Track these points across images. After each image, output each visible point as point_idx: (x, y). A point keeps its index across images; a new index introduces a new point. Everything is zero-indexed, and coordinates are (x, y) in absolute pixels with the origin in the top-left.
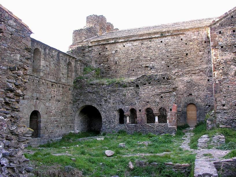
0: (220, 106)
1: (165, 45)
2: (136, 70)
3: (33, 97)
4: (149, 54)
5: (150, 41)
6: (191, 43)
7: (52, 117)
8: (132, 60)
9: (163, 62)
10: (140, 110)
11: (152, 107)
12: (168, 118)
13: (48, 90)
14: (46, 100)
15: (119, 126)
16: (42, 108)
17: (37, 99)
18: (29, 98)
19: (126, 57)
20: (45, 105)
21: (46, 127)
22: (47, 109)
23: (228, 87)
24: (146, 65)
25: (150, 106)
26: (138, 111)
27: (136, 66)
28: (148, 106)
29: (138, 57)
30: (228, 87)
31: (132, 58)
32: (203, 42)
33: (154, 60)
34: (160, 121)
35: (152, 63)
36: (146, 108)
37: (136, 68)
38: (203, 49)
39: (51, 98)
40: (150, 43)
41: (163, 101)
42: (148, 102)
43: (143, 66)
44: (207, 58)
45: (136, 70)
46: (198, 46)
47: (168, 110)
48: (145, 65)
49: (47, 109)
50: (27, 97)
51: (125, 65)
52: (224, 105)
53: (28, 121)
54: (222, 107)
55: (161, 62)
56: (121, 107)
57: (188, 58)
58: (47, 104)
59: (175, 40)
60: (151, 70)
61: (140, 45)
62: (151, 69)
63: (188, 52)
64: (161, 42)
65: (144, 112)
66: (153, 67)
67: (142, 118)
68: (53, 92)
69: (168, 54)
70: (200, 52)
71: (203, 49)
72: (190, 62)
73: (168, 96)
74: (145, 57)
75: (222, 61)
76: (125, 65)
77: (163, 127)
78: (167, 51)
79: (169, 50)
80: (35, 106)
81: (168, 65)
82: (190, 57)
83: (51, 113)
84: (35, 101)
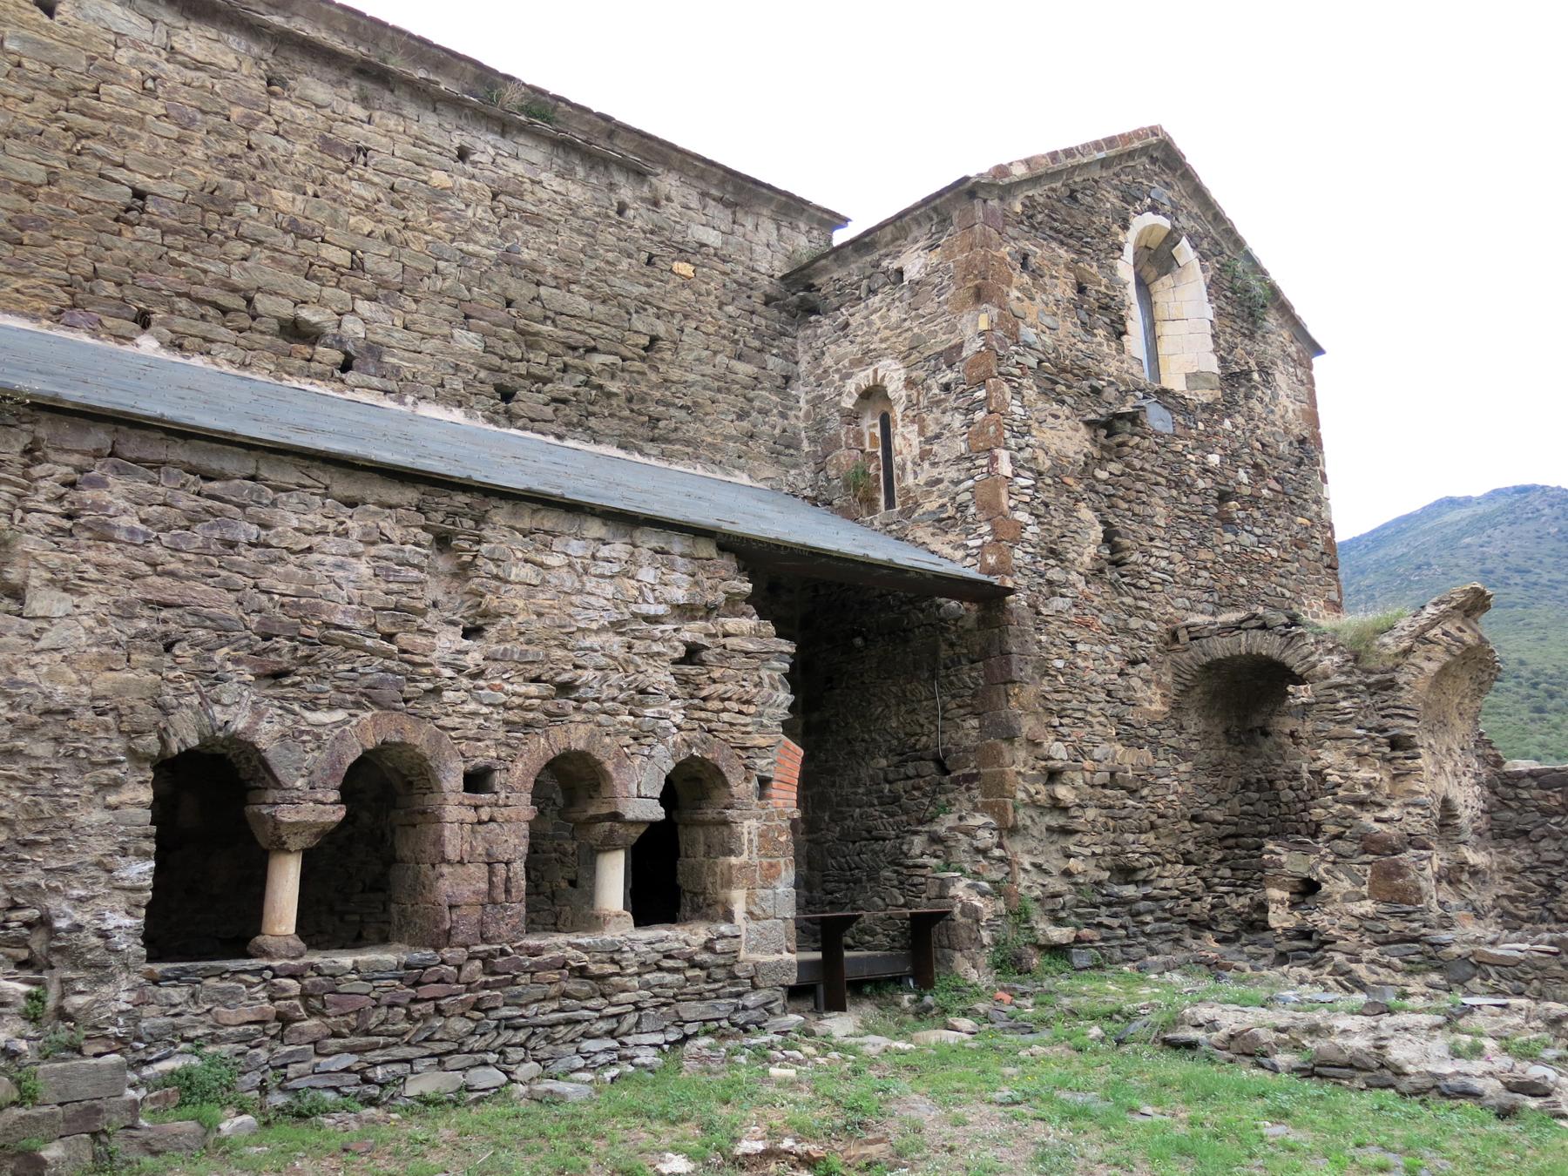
0: (1034, 780)
1: (495, 196)
2: (180, 323)
4: (343, 211)
5: (364, 101)
6: (685, 269)
8: (139, 194)
9: (468, 341)
10: (477, 781)
11: (605, 751)
12: (742, 867)
15: (178, 994)
19: (54, 128)
23: (1073, 643)
24: (306, 314)
25: (592, 735)
26: (452, 780)
27: (172, 279)
28: (575, 736)
29: (211, 198)
30: (1073, 643)
31: (141, 181)
32: (758, 298)
33: (384, 292)
34: (317, 925)
35: (363, 307)
36: (541, 748)
37: (183, 304)
38: (757, 344)
40: (358, 111)
41: (704, 699)
42: (565, 689)
43: (263, 303)
44: (780, 422)
45: (180, 323)
46: (730, 309)
47: (741, 788)
48: (286, 310)
51: (40, 224)
52: (1053, 776)
54: (1040, 786)
55: (446, 330)
56: (243, 711)
57: (653, 377)
59: (577, 193)
60: (351, 377)
61: (257, 86)
62: (346, 367)
63: (661, 328)
64: (463, 154)
65: (522, 808)
66: (374, 350)
67: (501, 869)
69: (513, 283)
70: (739, 357)
71: (757, 344)
72: (672, 411)
73: (751, 647)
74: (296, 229)
75: (1040, 454)
76: (40, 224)
77: (694, 965)
78: (508, 259)
79: (527, 255)
81: (506, 380)
82: (675, 374)
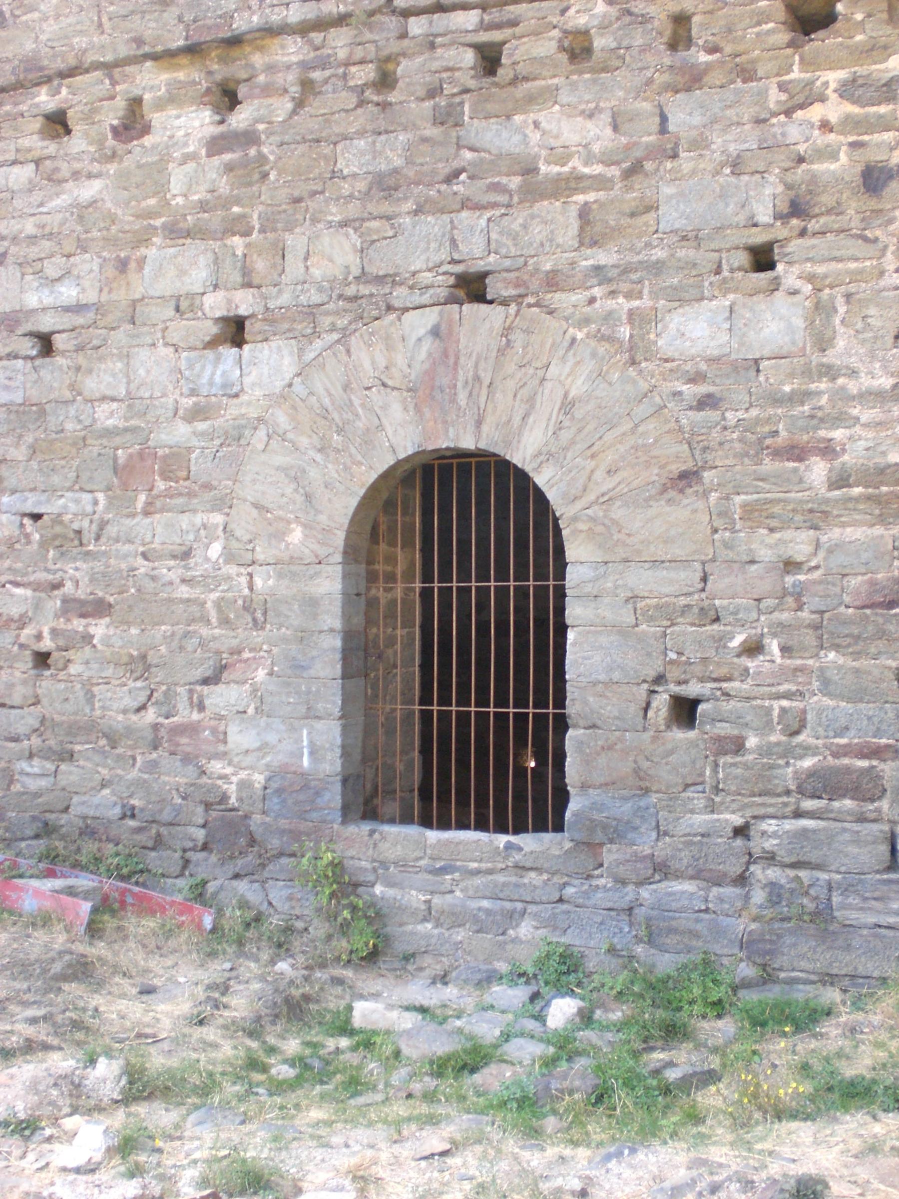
3: (380, 280)
7: (834, 534)
13: (684, 115)
14: (657, 268)
16: (568, 406)
17: (472, 288)
18: (311, 312)
20: (635, 354)
21: (693, 689)
22: (706, 402)
39: (796, 209)
49: (706, 402)
50: (285, 299)
53: (312, 603)
58: (695, 331)
68: (835, 109)
80: (427, 392)
83: (818, 471)
84: (419, 323)
